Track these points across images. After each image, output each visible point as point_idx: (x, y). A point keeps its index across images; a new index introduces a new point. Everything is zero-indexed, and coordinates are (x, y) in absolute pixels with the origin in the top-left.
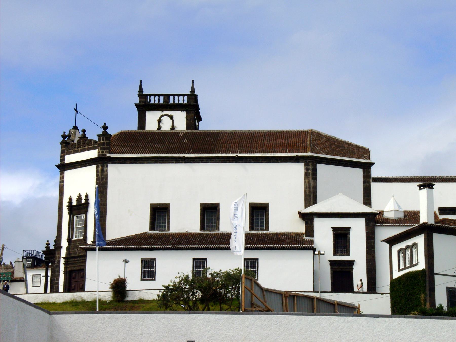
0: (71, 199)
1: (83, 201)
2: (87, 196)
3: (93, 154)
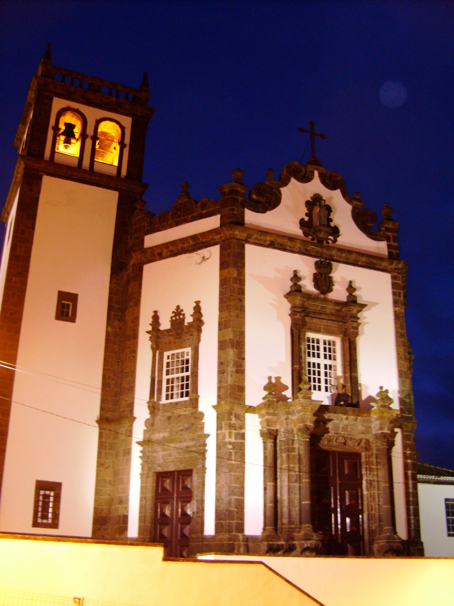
0: (156, 318)
1: (189, 319)
2: (197, 309)
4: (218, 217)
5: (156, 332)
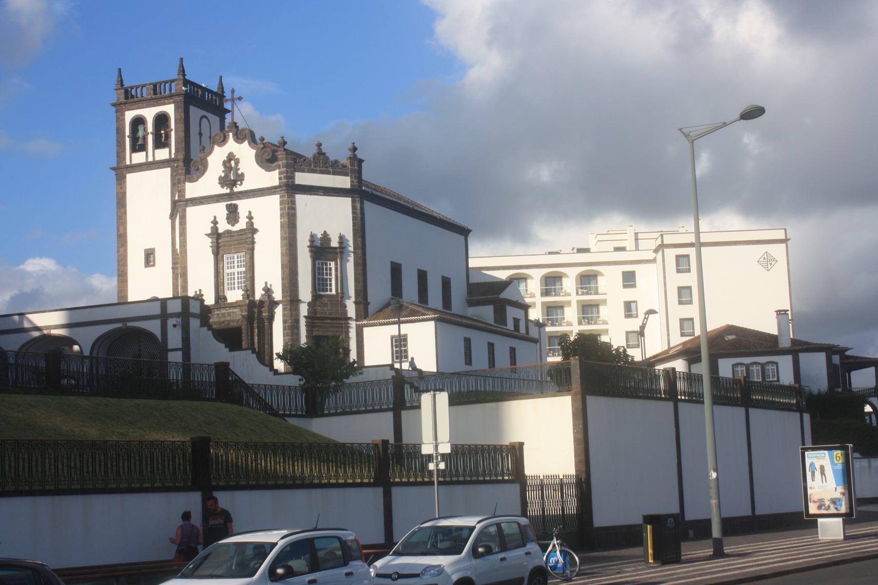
1: (334, 243)
2: (342, 238)
3: (344, 182)
4: (348, 179)
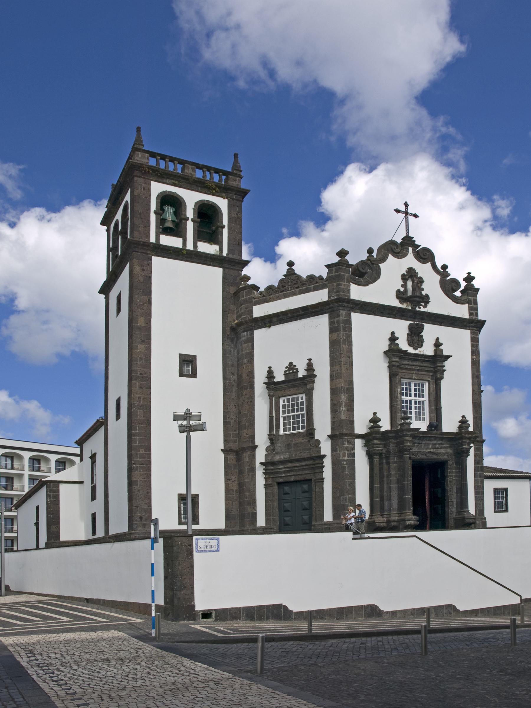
5: (271, 383)
